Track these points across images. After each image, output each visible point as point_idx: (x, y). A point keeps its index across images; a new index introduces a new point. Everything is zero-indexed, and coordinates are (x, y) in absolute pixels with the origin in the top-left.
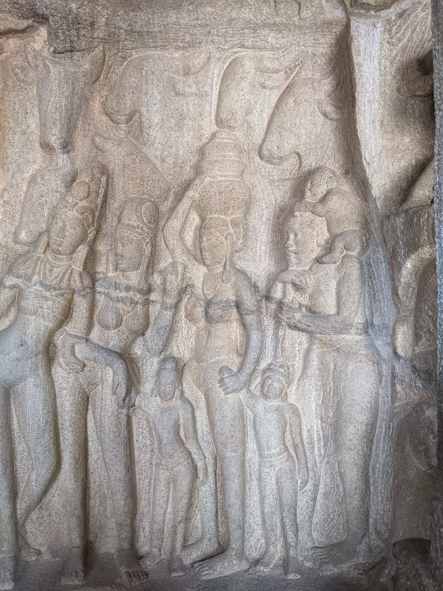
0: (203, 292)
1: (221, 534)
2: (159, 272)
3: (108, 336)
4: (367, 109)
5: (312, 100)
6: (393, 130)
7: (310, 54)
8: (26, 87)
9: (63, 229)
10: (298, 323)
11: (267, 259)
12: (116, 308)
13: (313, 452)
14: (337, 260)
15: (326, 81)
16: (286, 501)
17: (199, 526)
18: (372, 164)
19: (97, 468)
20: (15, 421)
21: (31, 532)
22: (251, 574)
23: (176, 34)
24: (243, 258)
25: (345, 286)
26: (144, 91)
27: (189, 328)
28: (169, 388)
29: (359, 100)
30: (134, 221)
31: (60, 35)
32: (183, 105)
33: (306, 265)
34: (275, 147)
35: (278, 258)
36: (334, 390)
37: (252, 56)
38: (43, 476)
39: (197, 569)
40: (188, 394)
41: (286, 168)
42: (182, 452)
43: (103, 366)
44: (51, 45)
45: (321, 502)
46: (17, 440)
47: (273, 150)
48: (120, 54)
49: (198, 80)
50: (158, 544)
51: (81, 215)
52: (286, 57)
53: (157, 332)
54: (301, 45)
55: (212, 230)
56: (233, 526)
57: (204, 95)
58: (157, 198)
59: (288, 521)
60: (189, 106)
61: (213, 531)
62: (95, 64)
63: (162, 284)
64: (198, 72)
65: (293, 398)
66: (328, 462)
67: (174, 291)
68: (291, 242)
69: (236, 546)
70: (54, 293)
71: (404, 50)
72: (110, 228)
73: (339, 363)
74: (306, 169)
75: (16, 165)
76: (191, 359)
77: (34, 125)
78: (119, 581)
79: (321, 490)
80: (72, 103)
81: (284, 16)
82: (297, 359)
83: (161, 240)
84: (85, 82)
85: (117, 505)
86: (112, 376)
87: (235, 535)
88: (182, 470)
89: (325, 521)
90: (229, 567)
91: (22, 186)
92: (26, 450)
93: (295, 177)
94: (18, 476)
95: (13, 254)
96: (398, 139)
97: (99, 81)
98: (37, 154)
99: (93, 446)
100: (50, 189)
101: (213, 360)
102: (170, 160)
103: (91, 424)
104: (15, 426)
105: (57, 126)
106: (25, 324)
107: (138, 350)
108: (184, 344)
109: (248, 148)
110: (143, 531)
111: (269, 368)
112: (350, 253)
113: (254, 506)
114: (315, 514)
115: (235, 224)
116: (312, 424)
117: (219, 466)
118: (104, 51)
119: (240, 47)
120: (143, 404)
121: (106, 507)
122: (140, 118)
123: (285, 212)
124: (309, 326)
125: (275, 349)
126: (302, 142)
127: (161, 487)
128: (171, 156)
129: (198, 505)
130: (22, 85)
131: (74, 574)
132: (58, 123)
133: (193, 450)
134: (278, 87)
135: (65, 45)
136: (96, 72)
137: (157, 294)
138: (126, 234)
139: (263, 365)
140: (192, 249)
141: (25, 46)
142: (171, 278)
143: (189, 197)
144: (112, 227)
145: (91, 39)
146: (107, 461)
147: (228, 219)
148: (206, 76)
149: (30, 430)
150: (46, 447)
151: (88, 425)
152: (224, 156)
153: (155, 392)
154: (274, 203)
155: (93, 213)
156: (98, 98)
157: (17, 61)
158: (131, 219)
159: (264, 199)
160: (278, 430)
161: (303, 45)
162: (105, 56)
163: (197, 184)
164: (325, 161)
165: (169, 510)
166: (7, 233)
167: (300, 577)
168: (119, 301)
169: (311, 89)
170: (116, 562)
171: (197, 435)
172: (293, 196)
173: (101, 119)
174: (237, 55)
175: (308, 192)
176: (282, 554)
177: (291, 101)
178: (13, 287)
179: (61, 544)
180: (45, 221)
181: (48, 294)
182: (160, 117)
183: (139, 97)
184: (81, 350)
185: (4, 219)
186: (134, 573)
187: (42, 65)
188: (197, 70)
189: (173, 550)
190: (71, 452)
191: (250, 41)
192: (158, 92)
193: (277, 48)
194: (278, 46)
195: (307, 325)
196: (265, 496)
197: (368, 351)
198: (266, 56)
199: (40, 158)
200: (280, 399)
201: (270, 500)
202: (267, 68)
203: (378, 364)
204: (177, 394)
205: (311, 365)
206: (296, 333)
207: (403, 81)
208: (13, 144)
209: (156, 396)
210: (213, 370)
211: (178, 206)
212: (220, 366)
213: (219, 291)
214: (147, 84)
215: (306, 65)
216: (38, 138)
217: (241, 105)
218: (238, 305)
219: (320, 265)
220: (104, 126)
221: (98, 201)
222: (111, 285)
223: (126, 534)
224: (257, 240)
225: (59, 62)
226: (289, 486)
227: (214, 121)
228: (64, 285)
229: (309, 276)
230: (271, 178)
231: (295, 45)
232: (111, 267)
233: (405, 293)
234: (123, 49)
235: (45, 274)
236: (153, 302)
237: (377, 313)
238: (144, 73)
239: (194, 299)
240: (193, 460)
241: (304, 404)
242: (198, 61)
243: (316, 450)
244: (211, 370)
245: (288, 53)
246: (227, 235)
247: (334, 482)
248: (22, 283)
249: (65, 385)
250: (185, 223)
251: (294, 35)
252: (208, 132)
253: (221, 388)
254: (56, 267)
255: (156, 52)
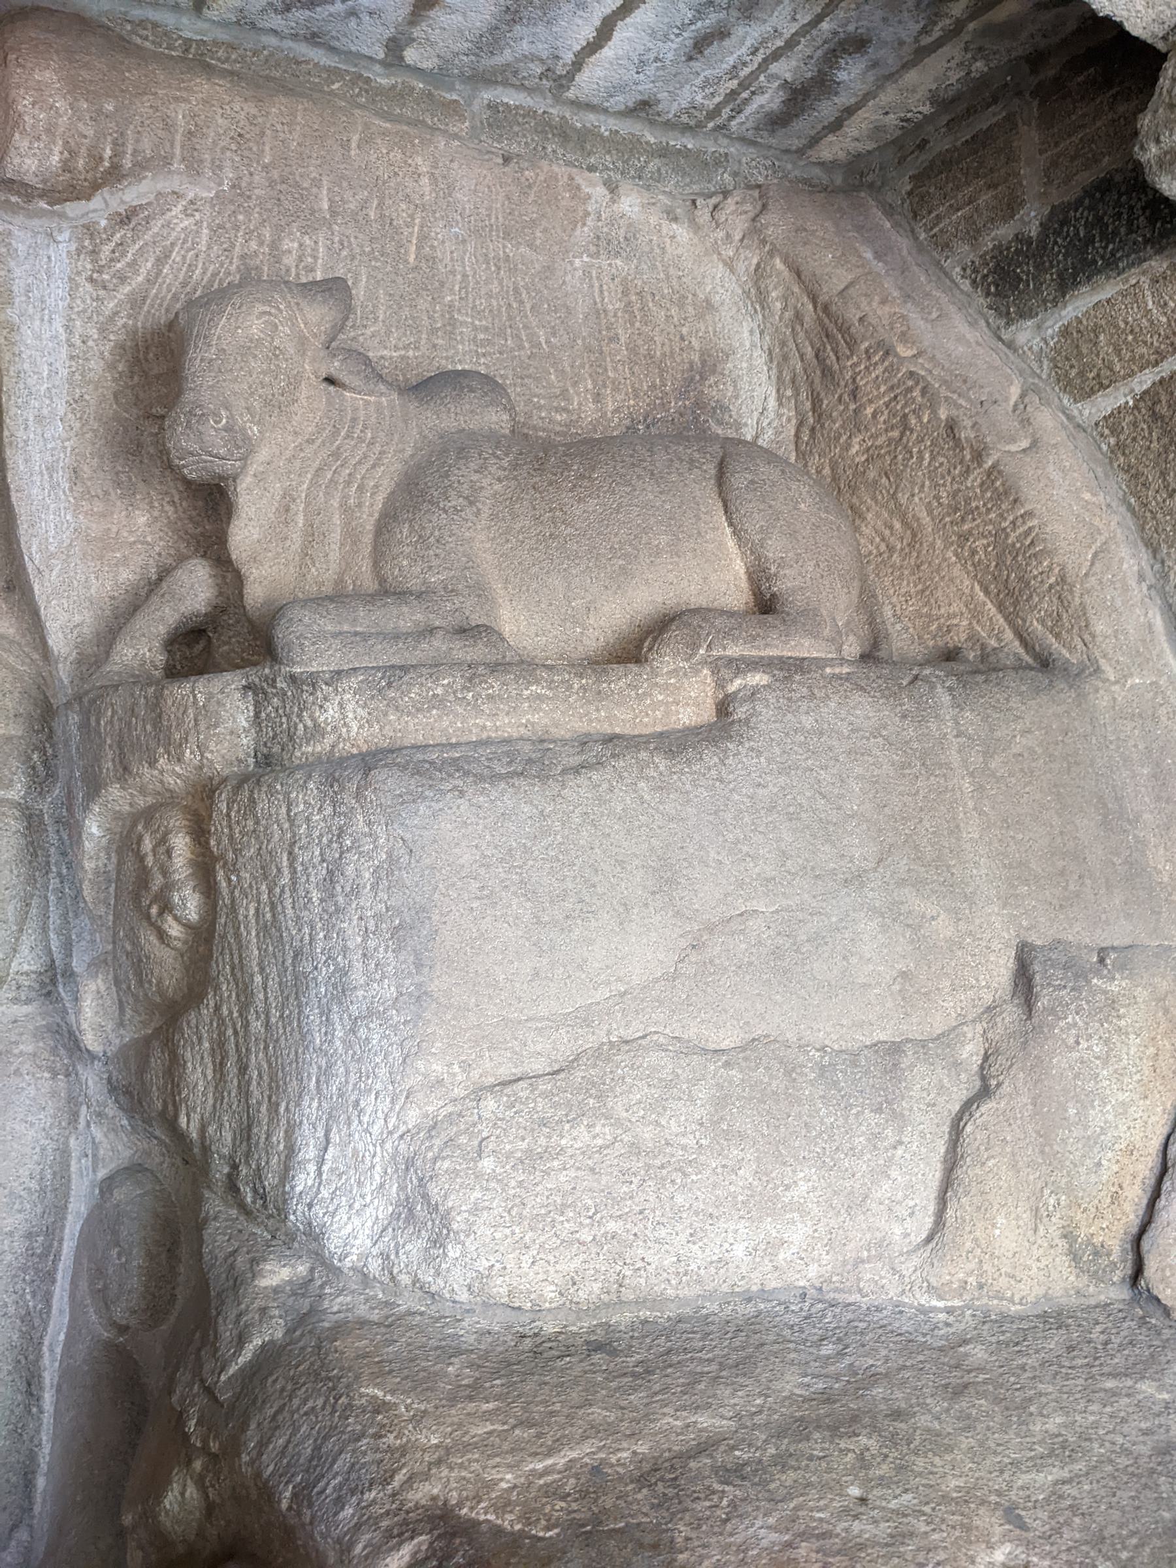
4: (32, 436)
6: (106, 493)
18: (46, 574)
29: (11, 413)
71: (136, 302)
96: (119, 516)
197: (41, 1044)
203: (67, 1075)
207: (132, 377)
233: (102, 896)
237: (83, 943)
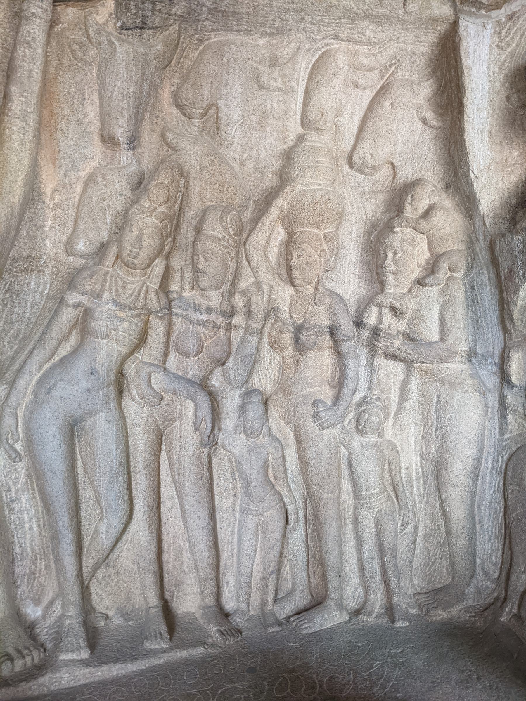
0: (291, 317)
1: (313, 585)
2: (240, 292)
3: (188, 365)
4: (475, 117)
5: (410, 104)
6: (501, 142)
7: (409, 53)
8: (84, 67)
9: (140, 238)
10: (397, 351)
11: (357, 280)
12: (197, 332)
13: (412, 492)
14: (441, 282)
15: (426, 84)
16: (388, 545)
17: (289, 577)
18: (480, 178)
19: (171, 517)
20: (79, 464)
21: (97, 594)
22: (354, 624)
23: (266, 17)
24: (331, 279)
25: (450, 310)
26: (224, 82)
27: (272, 358)
28: (256, 423)
29: (468, 107)
30: (219, 233)
31: (132, 7)
32: (266, 100)
33: (404, 288)
34: (369, 155)
35: (369, 280)
36: (437, 424)
37: (346, 50)
38: (115, 526)
39: (294, 623)
40: (275, 430)
41: (378, 179)
42: (273, 495)
43: (183, 399)
44: (118, 19)
45: (421, 545)
46: (81, 486)
47: (366, 158)
48: (197, 36)
49: (284, 72)
50: (246, 599)
51: (161, 222)
52: (383, 54)
53: (242, 361)
54: (400, 41)
55: (305, 245)
56: (331, 575)
57: (290, 90)
58: (238, 207)
59: (390, 566)
60: (273, 102)
61: (305, 582)
62: (169, 45)
63: (245, 307)
64: (285, 64)
65: (390, 434)
66: (427, 502)
67: (260, 314)
68: (389, 261)
69: (336, 595)
70: (130, 313)
71: (512, 55)
72: (185, 240)
73: (444, 394)
74: (402, 181)
75: (70, 162)
76: (275, 392)
77: (92, 114)
78: (210, 640)
79: (421, 532)
80: (141, 91)
81: (389, 8)
82: (393, 391)
83: (242, 256)
84: (156, 66)
85: (200, 557)
86: (192, 410)
87: (333, 584)
88: (273, 515)
89: (426, 565)
90: (330, 619)
91: (76, 187)
92: (92, 497)
93: (388, 189)
94: (83, 528)
95: (66, 267)
96: (506, 152)
97: (170, 67)
98: (96, 150)
99: (167, 492)
100: (113, 191)
101: (304, 393)
102: (250, 164)
103: (164, 466)
104: (79, 470)
105: (124, 117)
106: (94, 349)
107: (216, 382)
108: (266, 375)
109: (336, 155)
110: (227, 586)
111: (364, 401)
112: (454, 274)
113: (350, 553)
114: (415, 558)
115: (328, 239)
116: (411, 461)
117: (309, 511)
118: (179, 31)
119: (333, 39)
120: (227, 442)
121: (182, 562)
122: (217, 114)
123: (377, 228)
124: (410, 354)
125: (370, 380)
126: (398, 150)
127: (249, 535)
128: (251, 159)
129: (287, 555)
130: (80, 64)
131: (159, 636)
132: (125, 112)
133: (284, 493)
134: (371, 87)
135: (136, 20)
136: (169, 55)
137: (240, 318)
138: (210, 247)
139: (357, 398)
140: (276, 267)
141: (85, 17)
142: (256, 299)
143: (277, 206)
144: (187, 239)
145: (167, 15)
146: (187, 507)
147: (321, 233)
148: (294, 69)
149: (101, 474)
150: (119, 493)
151: (161, 468)
152: (317, 161)
153: (239, 428)
154: (364, 217)
155: (171, 221)
156: (168, 86)
157: (75, 35)
158: (214, 228)
159: (354, 212)
160: (378, 468)
161: (403, 41)
162: (179, 36)
163: (287, 192)
164: (423, 173)
165: (257, 561)
166: (57, 243)
167: (408, 624)
168: (200, 325)
169: (409, 92)
170: (202, 621)
171: (287, 476)
172: (386, 211)
173: (171, 111)
174: (328, 48)
175: (409, 206)
176: (383, 603)
177: (387, 103)
178: (77, 306)
179: (133, 606)
180: (107, 229)
181: (122, 314)
182: (240, 113)
183: (217, 88)
184: (159, 381)
185: (54, 225)
186: (226, 631)
187: (106, 42)
188: (285, 61)
189: (263, 604)
190: (145, 499)
191: (345, 32)
192: (240, 84)
193: (374, 42)
194: (375, 40)
195: (407, 353)
196: (363, 541)
197: (475, 381)
198: (361, 51)
199: (100, 154)
200: (377, 435)
201: (370, 543)
202: (362, 64)
203: (484, 395)
204: (265, 430)
205: (409, 397)
206: (391, 363)
207: (512, 90)
208: (66, 135)
209: (240, 434)
210: (305, 404)
211: (264, 218)
212: (313, 399)
213: (311, 315)
214: (228, 73)
215: (404, 65)
216: (97, 130)
217: (333, 105)
218: (332, 331)
219: (421, 287)
220: (175, 120)
221: (176, 208)
222: (189, 306)
223: (210, 589)
224: (346, 259)
225: (126, 40)
226: (391, 528)
227: (299, 121)
228: (140, 304)
229: (409, 300)
230: (361, 189)
231: (394, 40)
232: (187, 285)
233: (520, 317)
234: (201, 30)
235: (117, 291)
236: (235, 326)
237: (481, 340)
238: (225, 60)
239: (280, 324)
240: (284, 503)
241: (402, 440)
242: (287, 52)
243: (415, 489)
244: (303, 404)
245: (386, 49)
246: (321, 252)
247: (435, 523)
248: (88, 301)
249: (138, 422)
250: (269, 237)
251: (395, 30)
252: (293, 133)
253: (315, 422)
254: (130, 283)
255: (239, 37)
